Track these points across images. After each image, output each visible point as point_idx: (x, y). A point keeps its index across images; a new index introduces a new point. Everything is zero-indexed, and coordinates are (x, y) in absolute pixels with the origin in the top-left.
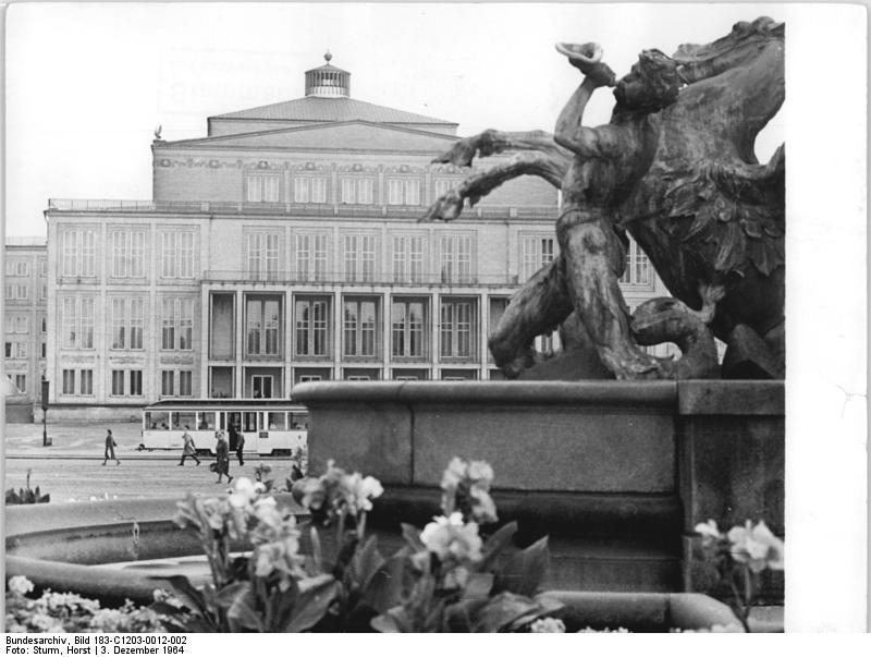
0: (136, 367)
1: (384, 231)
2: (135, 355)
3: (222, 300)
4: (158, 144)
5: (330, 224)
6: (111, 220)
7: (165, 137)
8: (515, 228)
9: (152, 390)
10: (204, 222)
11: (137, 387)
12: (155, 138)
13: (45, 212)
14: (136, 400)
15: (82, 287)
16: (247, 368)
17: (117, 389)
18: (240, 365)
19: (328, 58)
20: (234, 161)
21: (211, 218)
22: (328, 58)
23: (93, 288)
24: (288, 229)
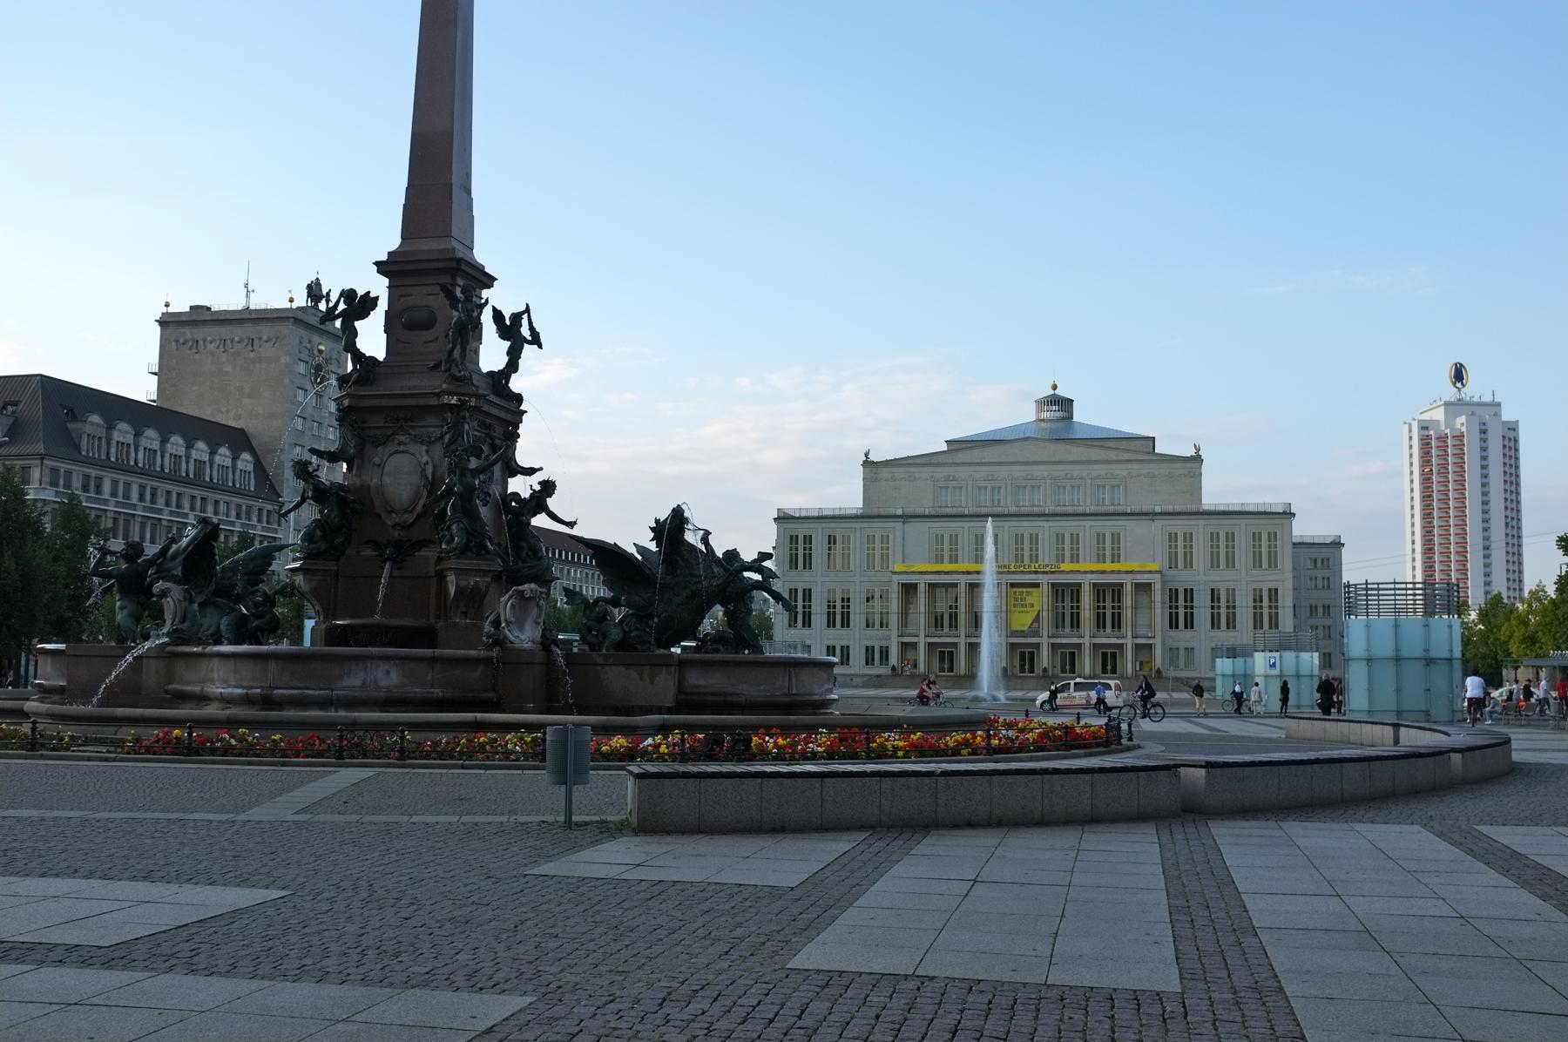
0: (845, 643)
3: (909, 590)
4: (867, 463)
7: (873, 458)
10: (899, 525)
18: (922, 641)
19: (1055, 387)
22: (1055, 387)
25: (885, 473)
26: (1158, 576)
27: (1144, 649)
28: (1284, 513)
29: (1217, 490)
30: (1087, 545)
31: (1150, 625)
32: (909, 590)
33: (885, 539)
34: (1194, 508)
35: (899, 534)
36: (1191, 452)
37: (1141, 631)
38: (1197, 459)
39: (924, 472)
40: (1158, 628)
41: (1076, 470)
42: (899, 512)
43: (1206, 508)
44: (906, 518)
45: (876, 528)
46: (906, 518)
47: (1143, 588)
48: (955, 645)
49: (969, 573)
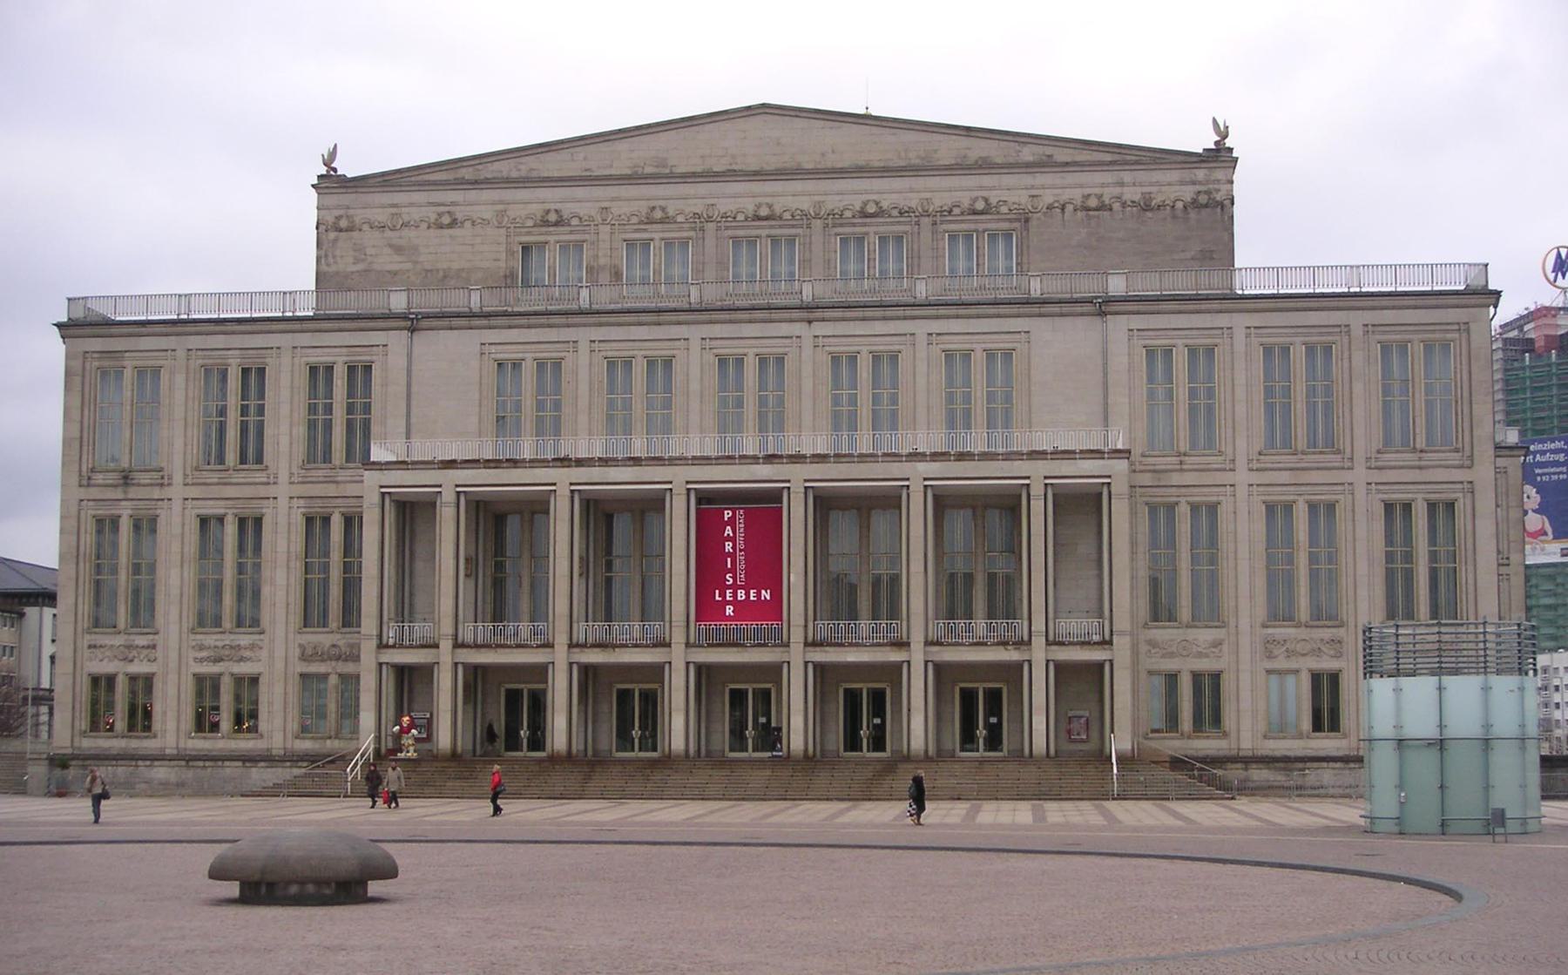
1: (807, 343)
2: (244, 640)
3: (411, 514)
4: (330, 183)
5: (682, 331)
6: (195, 342)
7: (348, 167)
8: (1119, 325)
9: (278, 725)
10: (396, 340)
11: (246, 719)
12: (323, 170)
13: (59, 326)
14: (245, 744)
15: (133, 492)
16: (816, 666)
17: (204, 722)
20: (487, 213)
21: (412, 330)
23: (156, 493)
24: (584, 347)
25: (376, 207)
26: (1121, 466)
27: (1082, 683)
28: (1469, 292)
29: (1272, 244)
30: (922, 377)
31: (1100, 608)
32: (411, 514)
33: (360, 374)
34: (1208, 282)
35: (397, 360)
36: (1200, 140)
37: (1072, 625)
38: (1220, 156)
39: (481, 203)
40: (1122, 622)
41: (891, 192)
42: (398, 302)
43: (1247, 285)
44: (412, 323)
45: (335, 348)
46: (412, 323)
47: (1080, 507)
48: (540, 672)
49: (580, 463)
